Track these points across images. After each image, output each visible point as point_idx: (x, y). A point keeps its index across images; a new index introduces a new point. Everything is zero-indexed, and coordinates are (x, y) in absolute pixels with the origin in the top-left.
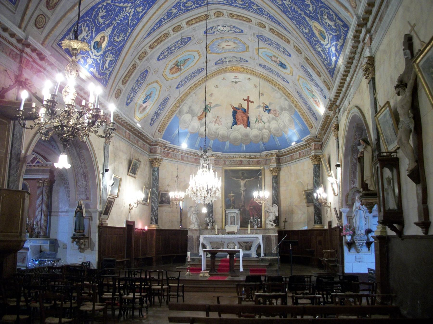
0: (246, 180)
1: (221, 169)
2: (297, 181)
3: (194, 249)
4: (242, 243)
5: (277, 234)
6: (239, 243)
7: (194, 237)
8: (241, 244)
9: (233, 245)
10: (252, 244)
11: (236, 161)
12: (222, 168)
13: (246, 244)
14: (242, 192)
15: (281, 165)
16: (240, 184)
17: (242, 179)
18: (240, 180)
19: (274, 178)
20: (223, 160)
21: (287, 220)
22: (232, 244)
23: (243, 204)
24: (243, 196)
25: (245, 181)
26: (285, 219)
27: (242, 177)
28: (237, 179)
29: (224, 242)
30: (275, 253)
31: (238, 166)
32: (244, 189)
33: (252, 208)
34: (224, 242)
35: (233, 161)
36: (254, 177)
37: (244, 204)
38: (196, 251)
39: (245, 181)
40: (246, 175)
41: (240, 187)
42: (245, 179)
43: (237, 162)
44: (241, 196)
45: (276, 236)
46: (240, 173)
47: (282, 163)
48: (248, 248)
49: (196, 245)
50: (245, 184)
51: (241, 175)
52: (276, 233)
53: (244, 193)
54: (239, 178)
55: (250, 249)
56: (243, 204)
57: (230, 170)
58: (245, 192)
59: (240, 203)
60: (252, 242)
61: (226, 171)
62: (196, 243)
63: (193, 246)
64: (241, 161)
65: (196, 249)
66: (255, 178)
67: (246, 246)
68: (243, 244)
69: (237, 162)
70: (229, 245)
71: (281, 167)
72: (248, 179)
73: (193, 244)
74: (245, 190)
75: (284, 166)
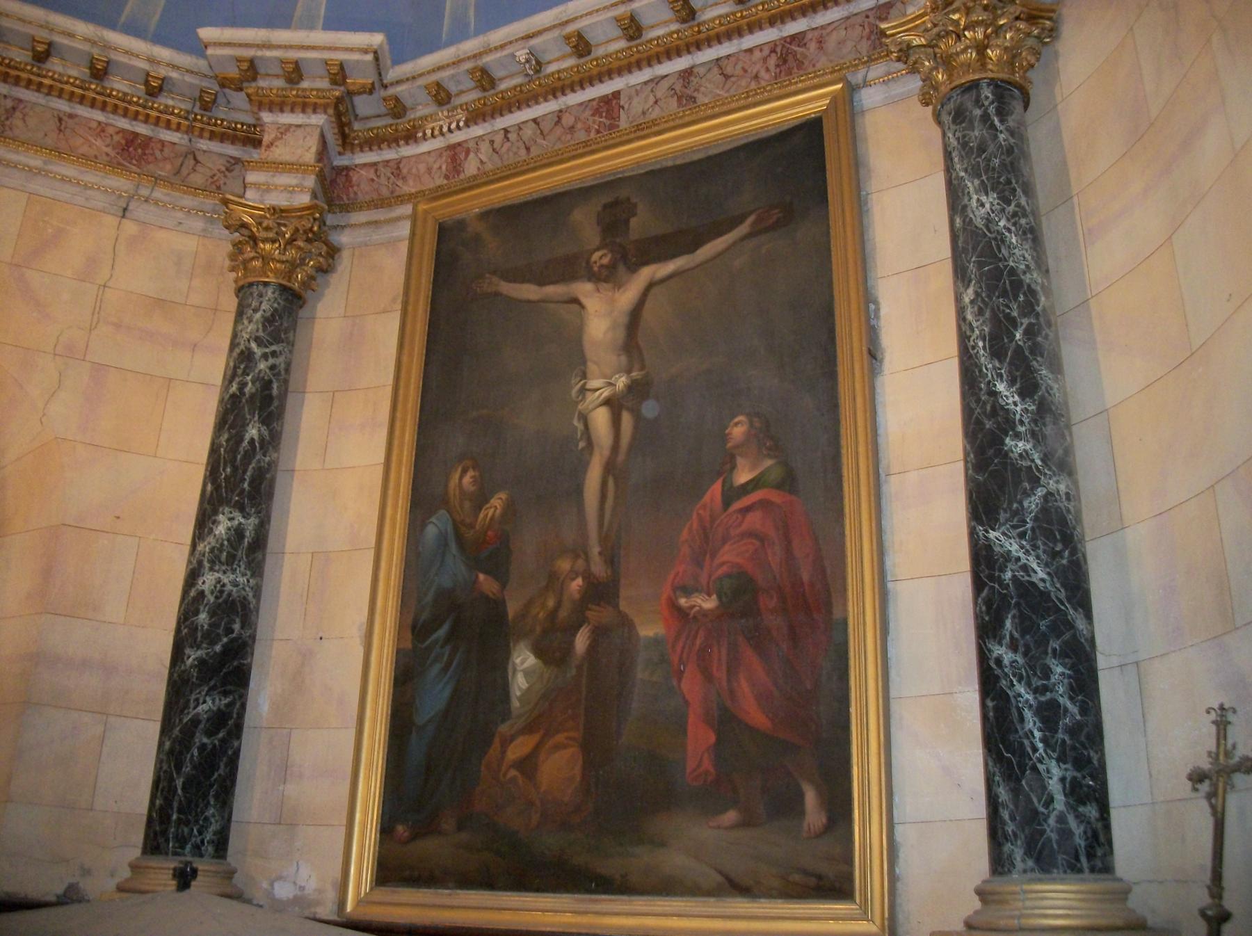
0: (647, 273)
11: (560, 114)
14: (601, 419)
16: (580, 329)
18: (583, 289)
19: (959, 116)
20: (438, 143)
23: (599, 568)
24: (609, 468)
25: (628, 296)
27: (601, 258)
28: (550, 290)
32: (621, 382)
33: (709, 604)
35: (528, 132)
37: (611, 560)
40: (642, 224)
42: (633, 268)
43: (568, 120)
46: (585, 220)
50: (635, 315)
53: (616, 422)
56: (599, 568)
59: (564, 565)
64: (610, 104)
66: (743, 229)
69: (568, 120)
74: (631, 388)
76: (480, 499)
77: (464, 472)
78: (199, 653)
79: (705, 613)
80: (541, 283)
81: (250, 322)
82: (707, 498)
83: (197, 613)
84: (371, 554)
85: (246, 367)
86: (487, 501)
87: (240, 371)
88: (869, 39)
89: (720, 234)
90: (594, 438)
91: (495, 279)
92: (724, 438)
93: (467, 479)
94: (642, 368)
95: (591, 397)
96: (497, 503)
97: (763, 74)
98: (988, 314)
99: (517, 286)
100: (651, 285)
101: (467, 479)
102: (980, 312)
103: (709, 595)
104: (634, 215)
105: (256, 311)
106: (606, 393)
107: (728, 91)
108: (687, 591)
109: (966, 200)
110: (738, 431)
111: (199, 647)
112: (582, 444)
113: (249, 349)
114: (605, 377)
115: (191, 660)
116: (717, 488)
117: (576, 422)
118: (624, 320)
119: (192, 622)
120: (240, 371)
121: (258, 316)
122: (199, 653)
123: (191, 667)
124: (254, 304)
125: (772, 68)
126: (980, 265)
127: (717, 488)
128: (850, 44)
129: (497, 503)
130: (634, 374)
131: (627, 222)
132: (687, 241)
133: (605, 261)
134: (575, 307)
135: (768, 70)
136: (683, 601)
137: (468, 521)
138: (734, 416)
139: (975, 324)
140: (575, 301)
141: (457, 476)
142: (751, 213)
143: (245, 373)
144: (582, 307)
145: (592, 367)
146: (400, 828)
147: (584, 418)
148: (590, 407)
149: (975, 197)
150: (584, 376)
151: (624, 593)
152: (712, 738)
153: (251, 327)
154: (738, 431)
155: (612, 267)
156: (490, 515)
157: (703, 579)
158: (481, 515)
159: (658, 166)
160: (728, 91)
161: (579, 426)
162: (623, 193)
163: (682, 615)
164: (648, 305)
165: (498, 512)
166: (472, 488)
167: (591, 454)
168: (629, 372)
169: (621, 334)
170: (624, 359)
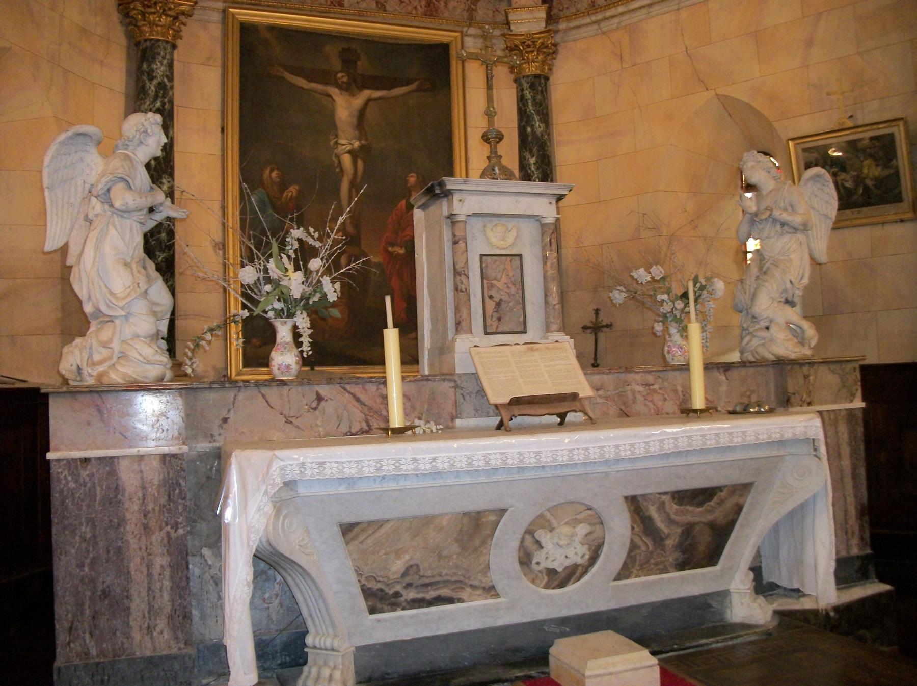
0: (367, 93)
1: (216, 17)
2: (701, 98)
3: (138, 605)
4: (662, 507)
5: (859, 403)
6: (635, 504)
7: (128, 478)
8: (653, 511)
9: (582, 530)
10: (739, 509)
12: (225, 11)
13: (695, 514)
14: (347, 160)
15: (563, 26)
17: (346, 88)
18: (334, 91)
21: (604, 319)
22: (575, 522)
25: (359, 101)
26: (597, 312)
28: (314, 85)
29: (502, 512)
30: (855, 551)
31: (323, 14)
32: (357, 144)
34: (502, 512)
36: (409, 82)
38: (161, 623)
39: (359, 101)
40: (363, 66)
41: (332, 126)
44: (341, 181)
45: (851, 412)
46: (332, 52)
47: (569, 18)
48: (704, 539)
49: (161, 561)
50: (362, 113)
51: (337, 64)
52: (851, 397)
54: (326, 77)
55: (712, 557)
57: (272, 28)
58: (360, 163)
60: (746, 487)
61: (247, 30)
62: (157, 537)
63: (124, 573)
65: (165, 601)
66: (414, 86)
67: (688, 530)
68: (672, 507)
70: (543, 536)
71: (558, 38)
72: (377, 88)
73: (119, 553)
74: (362, 147)
75: (584, 32)
76: (283, 186)
77: (272, 171)
78: (165, 255)
79: (398, 254)
80: (310, 79)
81: (162, 64)
82: (399, 206)
83: (160, 233)
84: (217, 206)
85: (164, 94)
86: (287, 188)
87: (160, 95)
88: (467, 11)
89: (402, 85)
90: (344, 167)
91: (281, 69)
92: (407, 182)
93: (274, 174)
94: (367, 140)
95: (340, 148)
96: (293, 190)
97: (418, 7)
98: (540, 170)
99: (295, 77)
100: (369, 100)
101: (274, 174)
102: (537, 169)
103: (402, 247)
104: (359, 60)
105: (164, 58)
106: (349, 148)
107: (402, 9)
108: (393, 245)
109: (534, 123)
110: (412, 179)
111: (164, 252)
112: (337, 170)
113: (163, 82)
114: (348, 139)
115: (160, 258)
116: (403, 202)
117: (334, 159)
118: (356, 113)
119: (158, 238)
120: (160, 95)
121: (165, 62)
122: (165, 255)
123: (162, 262)
124: (162, 53)
125: (423, 6)
126: (538, 151)
127: (403, 202)
128: (459, 11)
129: (293, 190)
130: (363, 142)
131: (356, 62)
132: (391, 84)
133: (345, 79)
134: (330, 99)
135: (421, 7)
136: (390, 249)
137: (277, 196)
138: (410, 173)
139: (535, 172)
140: (329, 96)
141: (268, 172)
142: (416, 80)
143: (164, 96)
144: (333, 100)
145: (340, 133)
146: (254, 341)
147: (338, 156)
148: (341, 153)
149: (538, 123)
150: (337, 136)
151: (363, 241)
152: (405, 305)
153: (163, 68)
154: (412, 179)
155: (349, 83)
156: (290, 195)
157: (399, 241)
158: (285, 195)
159: (371, 39)
160: (402, 9)
161: (336, 161)
162: (353, 46)
163: (390, 254)
164: (368, 110)
165: (294, 194)
166: (278, 180)
167: (343, 175)
168: (360, 140)
169: (355, 120)
170: (357, 132)
